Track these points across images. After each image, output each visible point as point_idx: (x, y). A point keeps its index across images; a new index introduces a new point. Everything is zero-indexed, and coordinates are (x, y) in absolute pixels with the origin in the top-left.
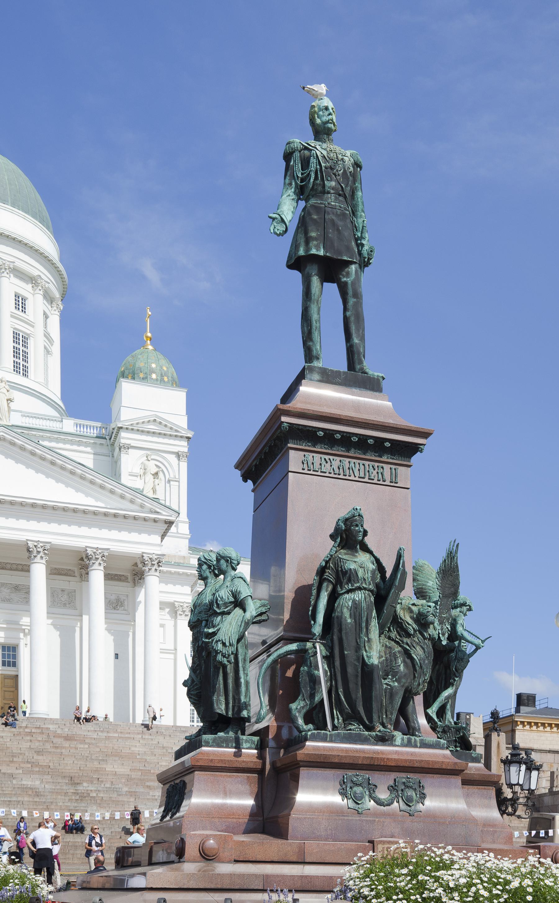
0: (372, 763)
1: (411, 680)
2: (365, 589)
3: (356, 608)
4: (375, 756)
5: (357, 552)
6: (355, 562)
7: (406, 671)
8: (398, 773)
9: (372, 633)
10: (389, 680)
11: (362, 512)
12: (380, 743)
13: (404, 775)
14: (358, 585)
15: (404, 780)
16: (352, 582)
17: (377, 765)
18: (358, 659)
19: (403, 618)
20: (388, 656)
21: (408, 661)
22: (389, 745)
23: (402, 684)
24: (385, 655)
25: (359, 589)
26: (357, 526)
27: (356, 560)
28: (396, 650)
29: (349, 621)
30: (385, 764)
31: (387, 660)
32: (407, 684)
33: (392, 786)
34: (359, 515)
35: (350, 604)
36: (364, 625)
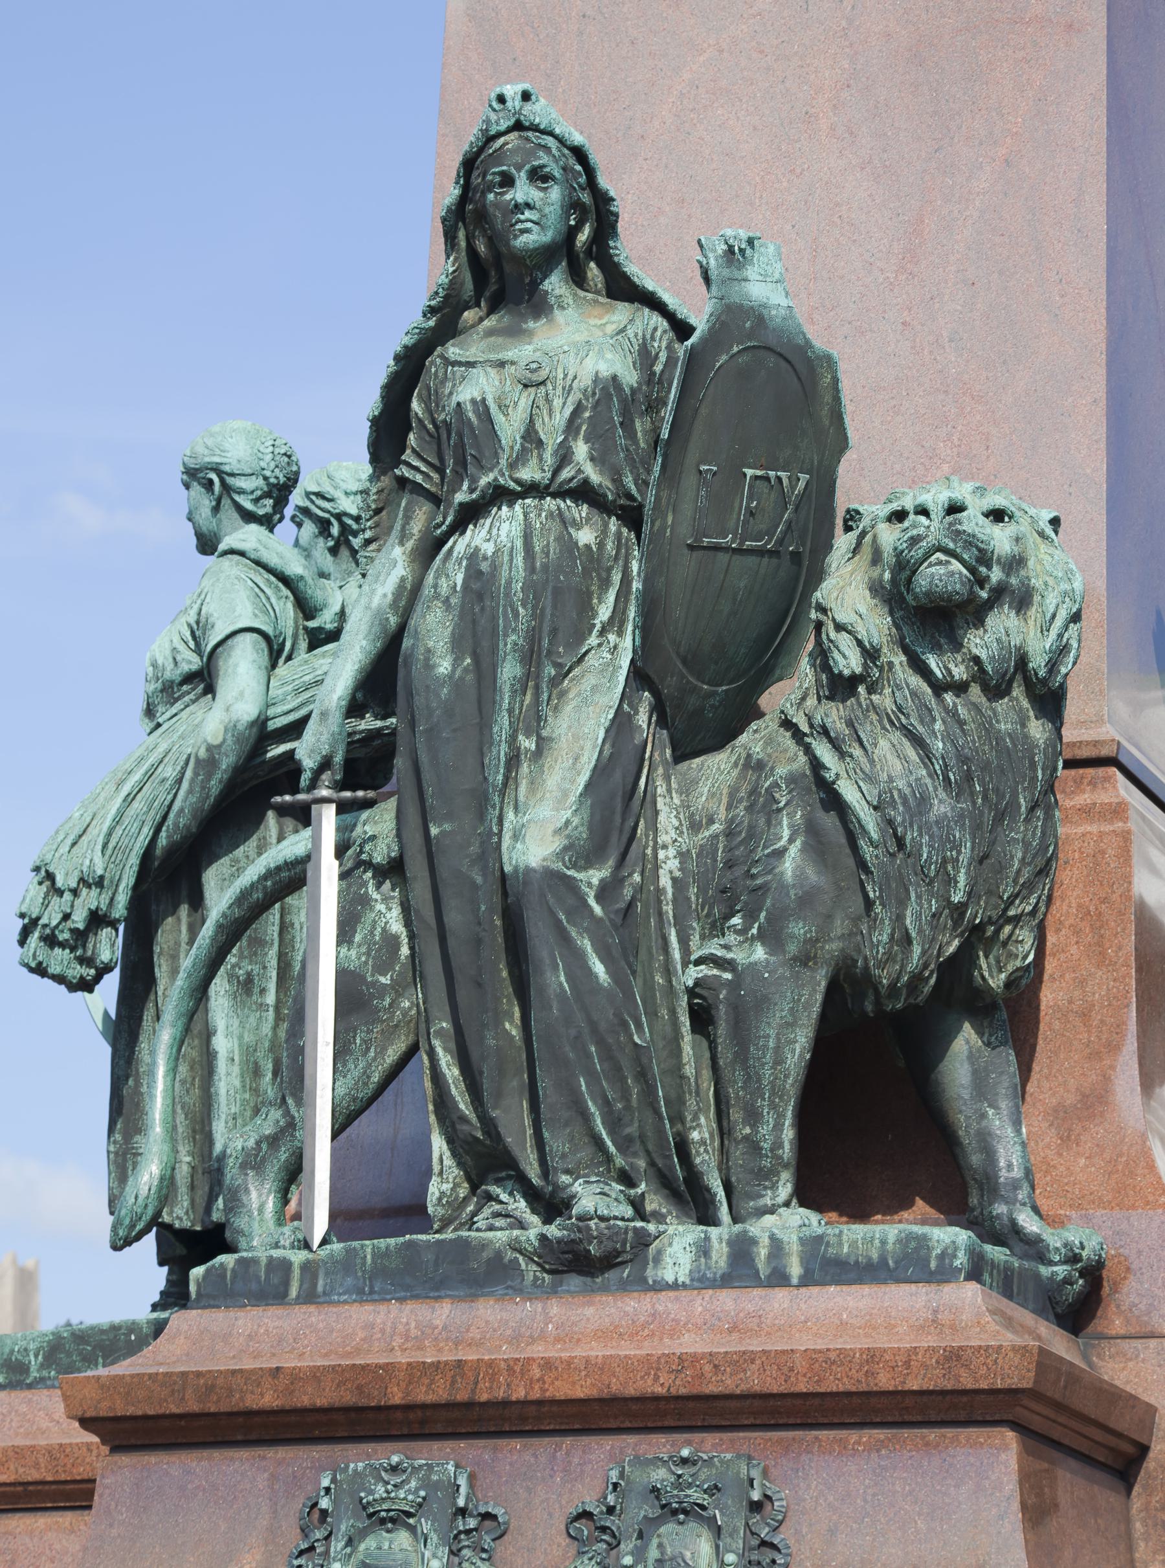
0: (462, 1396)
1: (856, 920)
2: (532, 490)
3: (480, 596)
4: (506, 1352)
5: (539, 306)
6: (501, 364)
7: (813, 875)
8: (631, 1439)
9: (568, 709)
10: (731, 938)
11: (540, 111)
12: (574, 1281)
13: (660, 1445)
14: (490, 477)
15: (660, 1476)
16: (471, 469)
17: (518, 1402)
18: (482, 858)
19: (830, 604)
20: (741, 811)
21: (829, 821)
22: (624, 1287)
23: (792, 949)
24: (729, 807)
25: (500, 495)
26: (508, 181)
27: (509, 355)
28: (782, 771)
29: (444, 666)
30: (536, 1395)
31: (729, 833)
32: (833, 947)
33: (586, 1515)
34: (518, 126)
35: (459, 579)
36: (509, 670)
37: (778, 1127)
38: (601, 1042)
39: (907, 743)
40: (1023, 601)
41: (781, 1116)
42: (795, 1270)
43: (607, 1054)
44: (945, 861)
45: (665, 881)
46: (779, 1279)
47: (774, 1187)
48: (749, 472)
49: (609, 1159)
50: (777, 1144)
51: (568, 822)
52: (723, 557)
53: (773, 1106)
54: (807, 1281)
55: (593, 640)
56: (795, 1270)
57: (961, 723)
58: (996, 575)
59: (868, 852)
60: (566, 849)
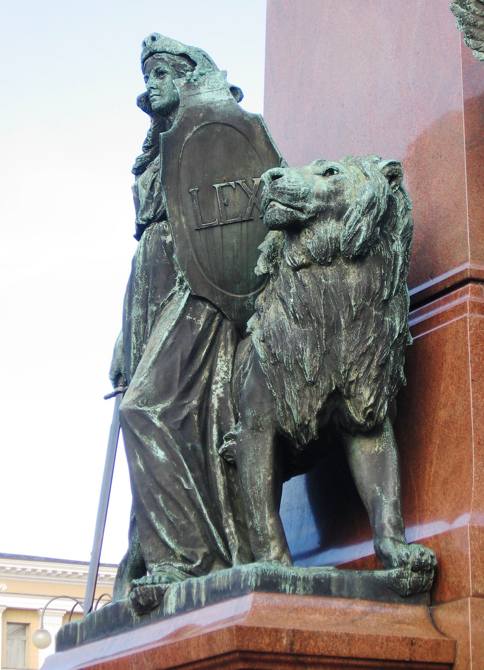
37: (263, 518)
38: (164, 492)
39: (280, 303)
40: (339, 214)
41: (263, 513)
42: (203, 599)
43: (168, 496)
44: (296, 362)
45: (215, 402)
46: (199, 606)
47: (269, 551)
48: (217, 186)
49: (173, 552)
50: (264, 528)
51: (142, 383)
52: (217, 230)
53: (257, 508)
54: (208, 603)
55: (176, 288)
56: (203, 599)
57: (304, 285)
58: (312, 205)
59: (262, 365)
60: (139, 397)
